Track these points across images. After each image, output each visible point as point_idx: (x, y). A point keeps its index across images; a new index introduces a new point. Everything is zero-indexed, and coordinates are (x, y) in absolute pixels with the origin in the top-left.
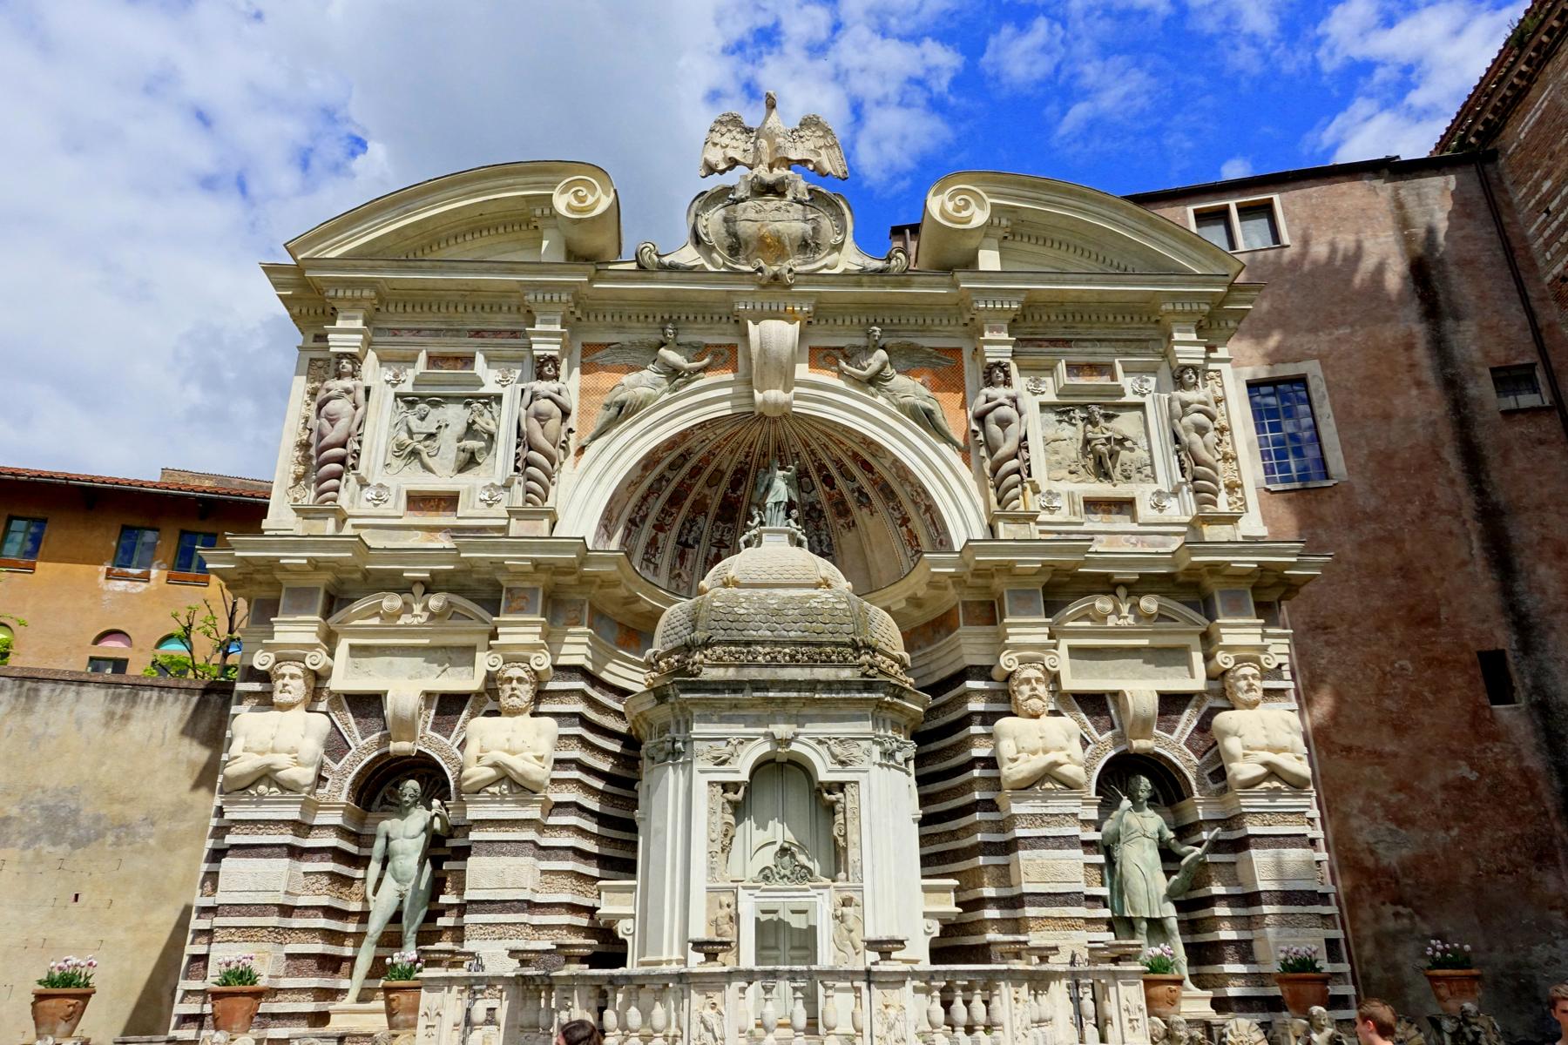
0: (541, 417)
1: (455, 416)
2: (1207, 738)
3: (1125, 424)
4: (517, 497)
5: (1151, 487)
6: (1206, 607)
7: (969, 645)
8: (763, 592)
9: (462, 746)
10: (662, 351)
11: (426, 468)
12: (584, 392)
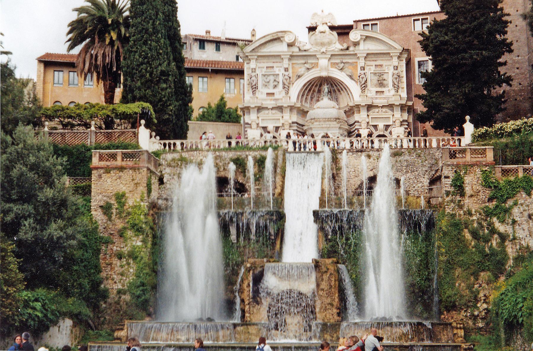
0: (286, 79)
1: (272, 78)
2: (391, 133)
3: (385, 77)
4: (283, 93)
5: (387, 89)
6: (393, 111)
7: (357, 117)
8: (322, 110)
9: (280, 135)
10: (305, 65)
11: (269, 88)
12: (293, 72)
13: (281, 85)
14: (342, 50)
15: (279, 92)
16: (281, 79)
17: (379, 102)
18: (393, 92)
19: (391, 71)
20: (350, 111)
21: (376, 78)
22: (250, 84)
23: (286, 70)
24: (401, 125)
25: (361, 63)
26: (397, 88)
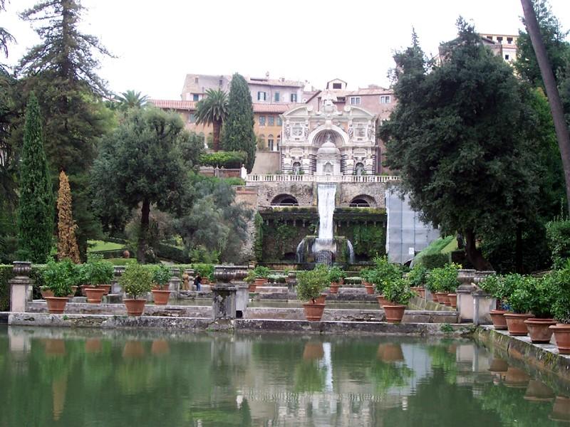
1: (298, 130)
3: (363, 130)
13: (303, 134)
14: (339, 115)
15: (302, 137)
16: (303, 131)
17: (360, 144)
18: (367, 139)
19: (367, 128)
20: (342, 149)
21: (358, 131)
22: (286, 133)
23: (307, 125)
24: (371, 157)
25: (350, 122)
26: (370, 137)
